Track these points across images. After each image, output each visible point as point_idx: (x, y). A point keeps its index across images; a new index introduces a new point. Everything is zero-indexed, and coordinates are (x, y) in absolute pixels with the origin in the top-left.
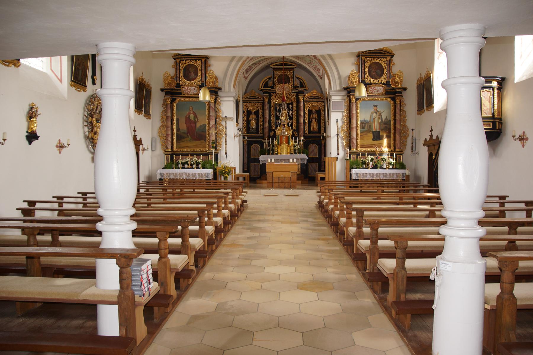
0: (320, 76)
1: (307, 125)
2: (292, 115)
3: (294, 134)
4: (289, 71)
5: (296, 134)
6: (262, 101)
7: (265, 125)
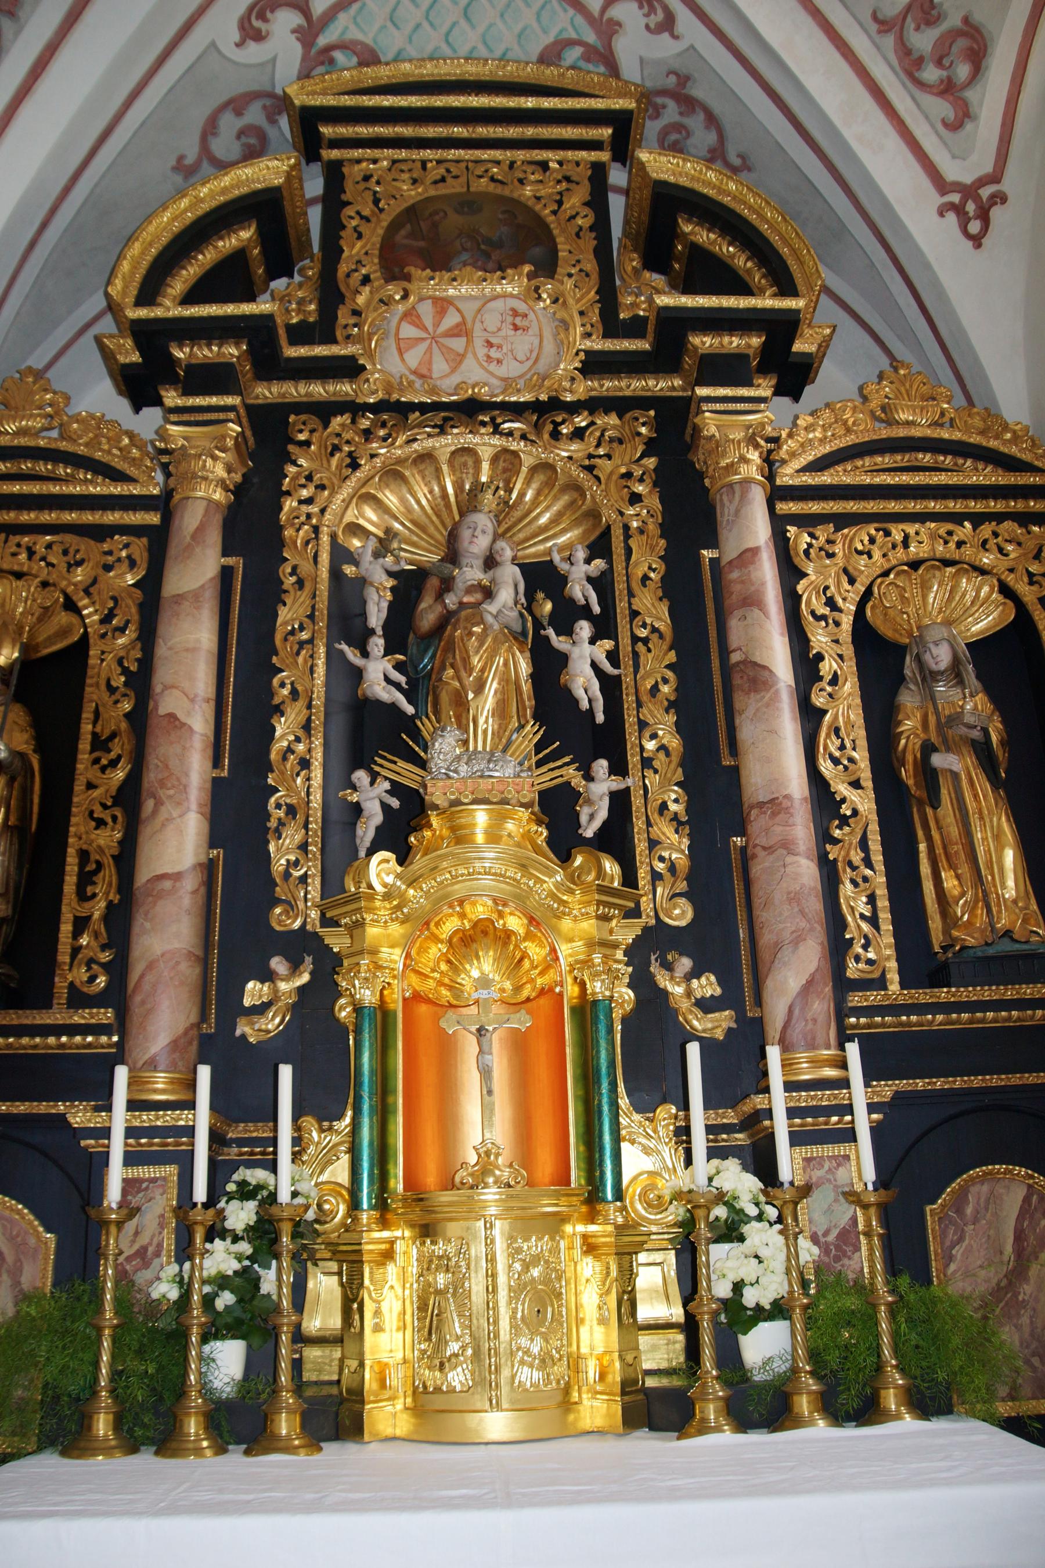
0: (969, 191)
1: (864, 844)
2: (610, 686)
3: (665, 994)
4: (544, 166)
5: (706, 1005)
6: (153, 518)
7: (146, 833)
